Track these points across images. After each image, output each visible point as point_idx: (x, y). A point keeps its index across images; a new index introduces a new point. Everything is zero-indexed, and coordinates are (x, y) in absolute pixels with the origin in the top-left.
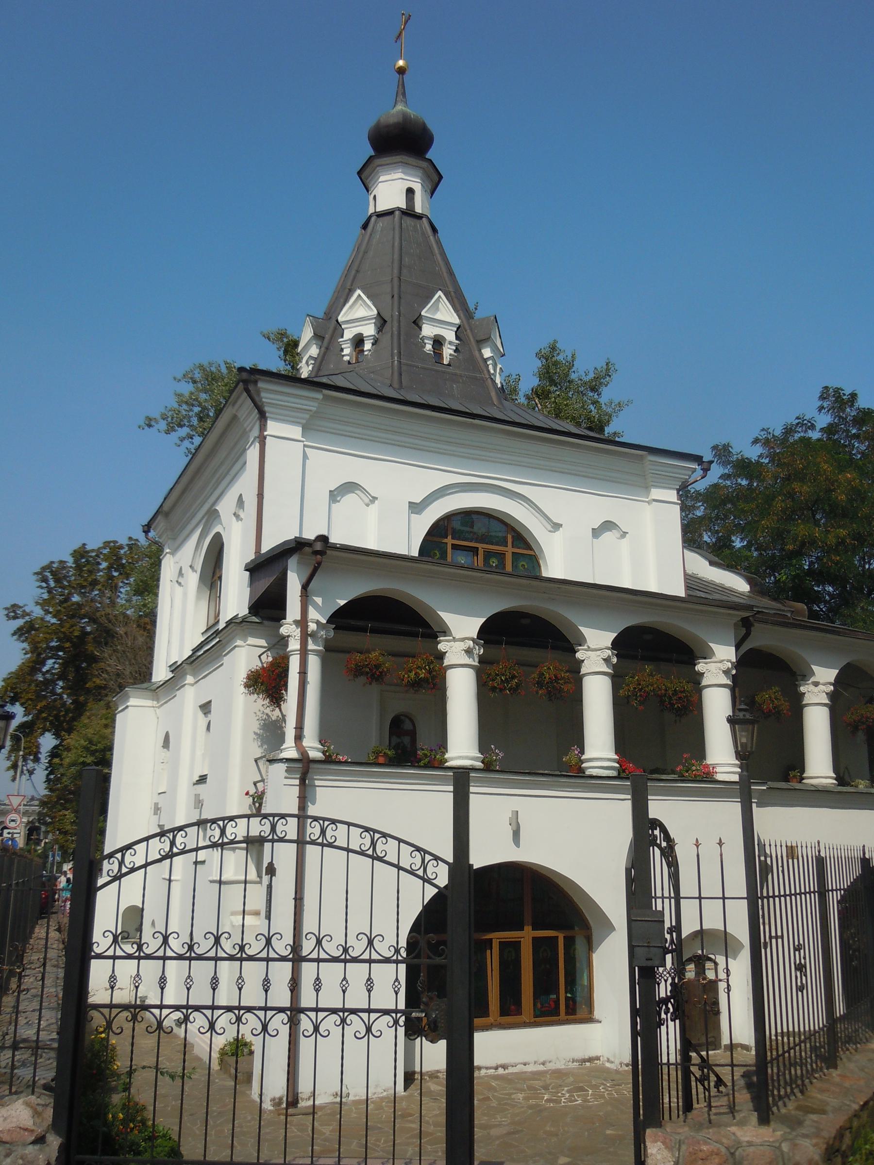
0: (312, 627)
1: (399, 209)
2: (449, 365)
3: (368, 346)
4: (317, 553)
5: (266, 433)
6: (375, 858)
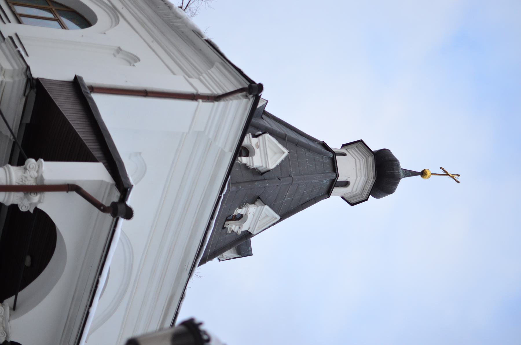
0: (35, 198)
1: (337, 176)
5: (200, 101)
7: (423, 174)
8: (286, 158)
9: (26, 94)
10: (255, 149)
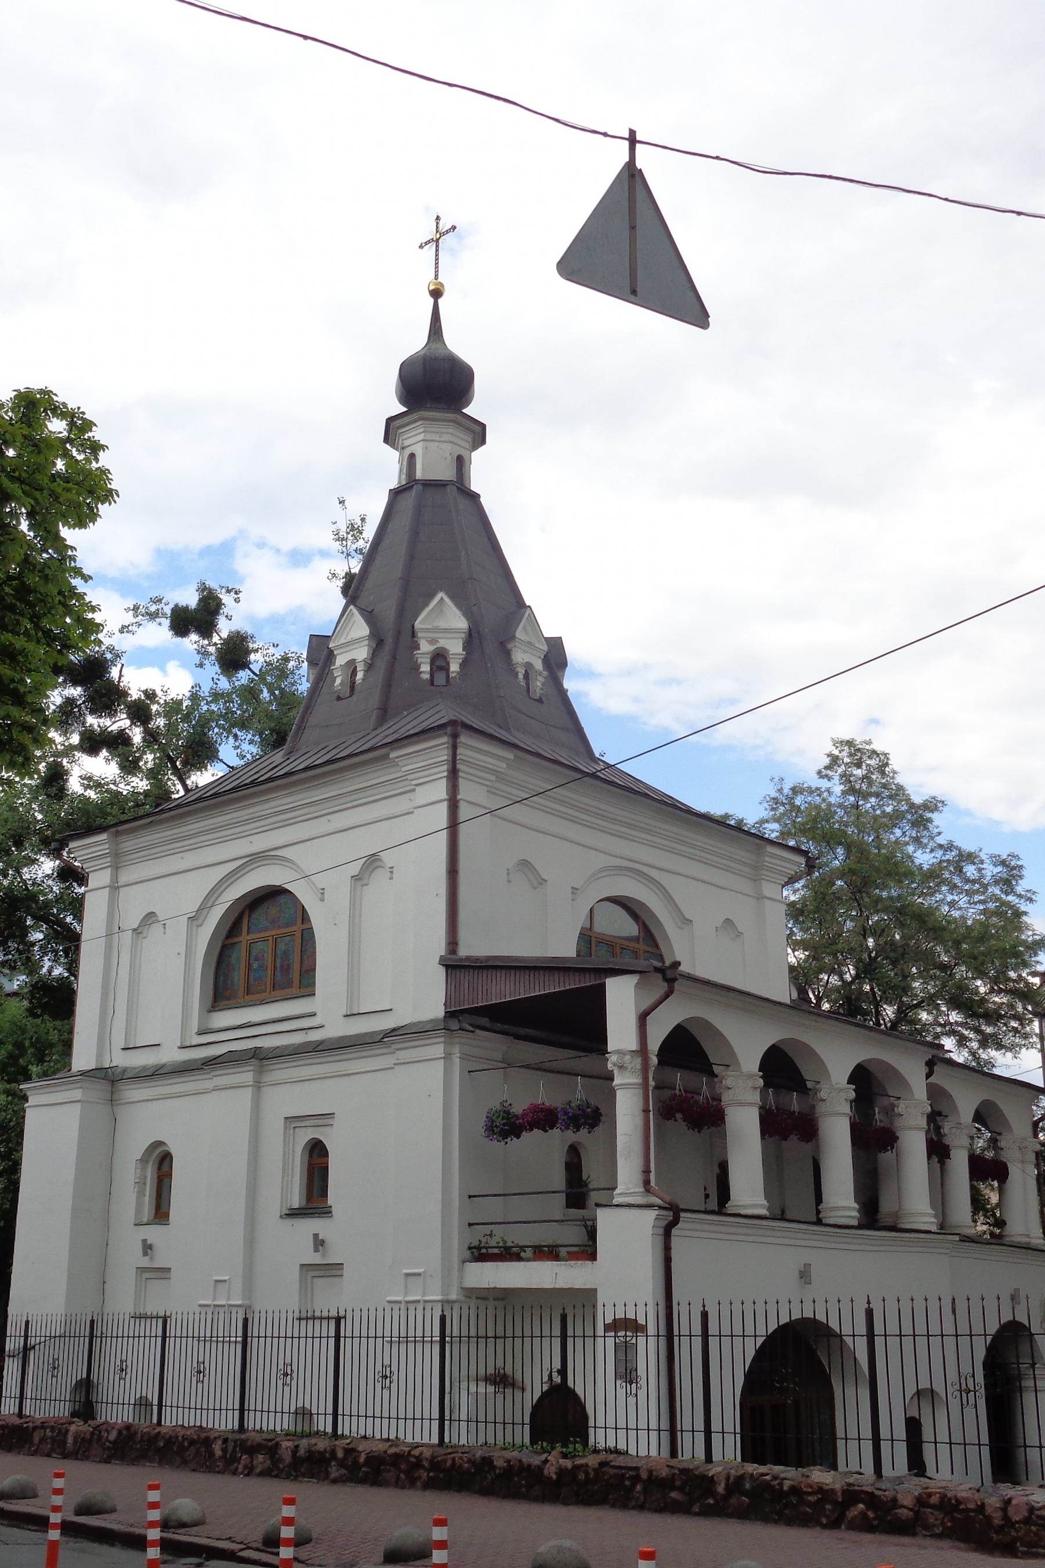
2: (540, 701)
3: (454, 667)
5: (459, 797)
7: (436, 294)
8: (451, 598)
9: (471, 1029)
10: (438, 645)
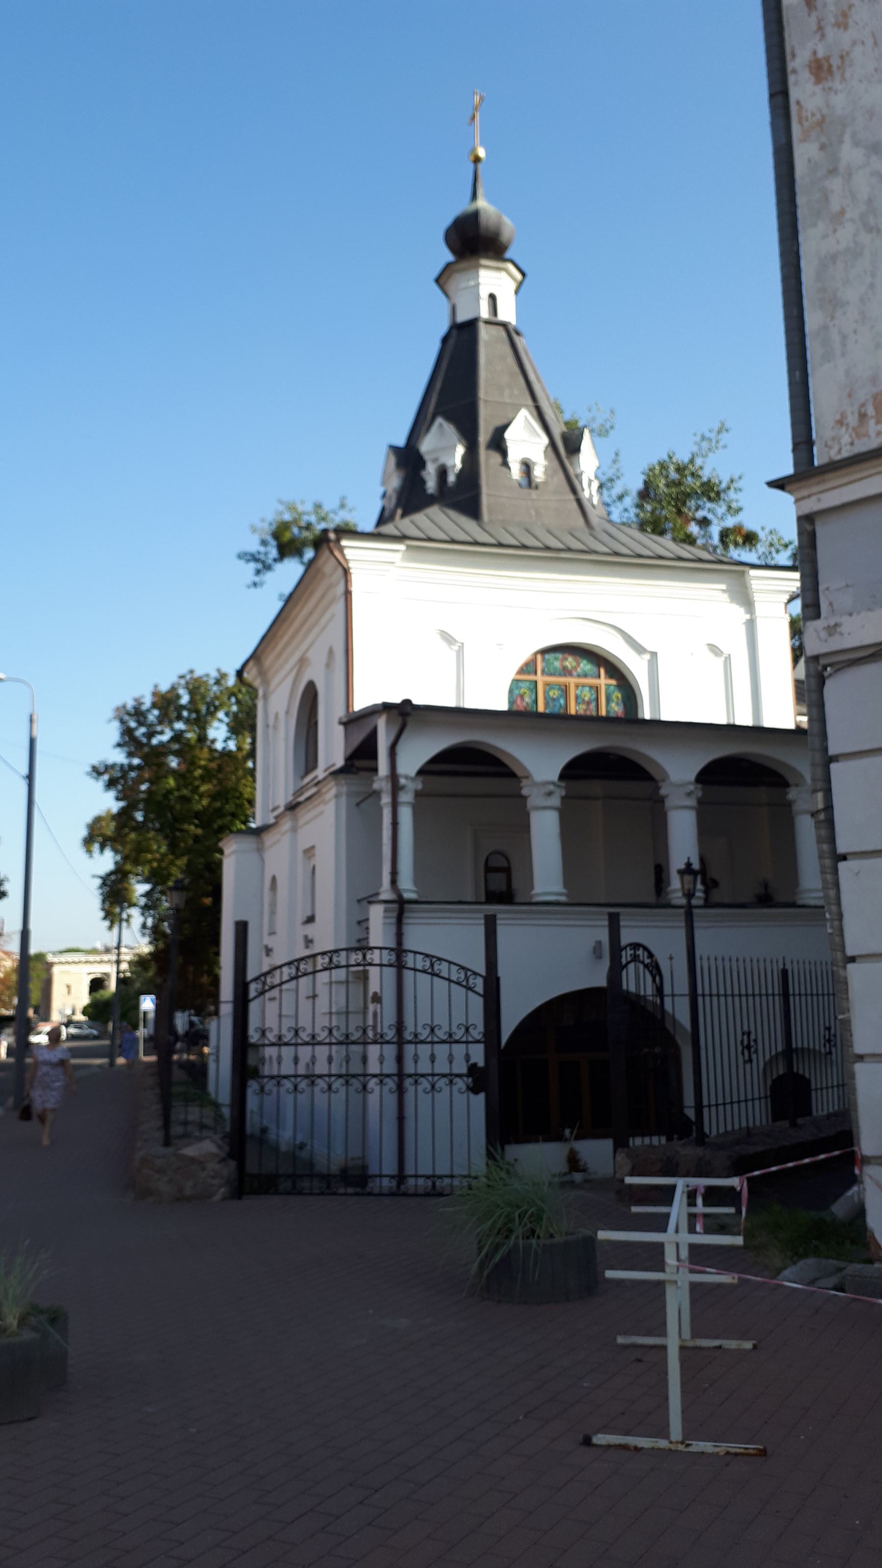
0: (402, 781)
4: (404, 714)
6: (434, 974)
